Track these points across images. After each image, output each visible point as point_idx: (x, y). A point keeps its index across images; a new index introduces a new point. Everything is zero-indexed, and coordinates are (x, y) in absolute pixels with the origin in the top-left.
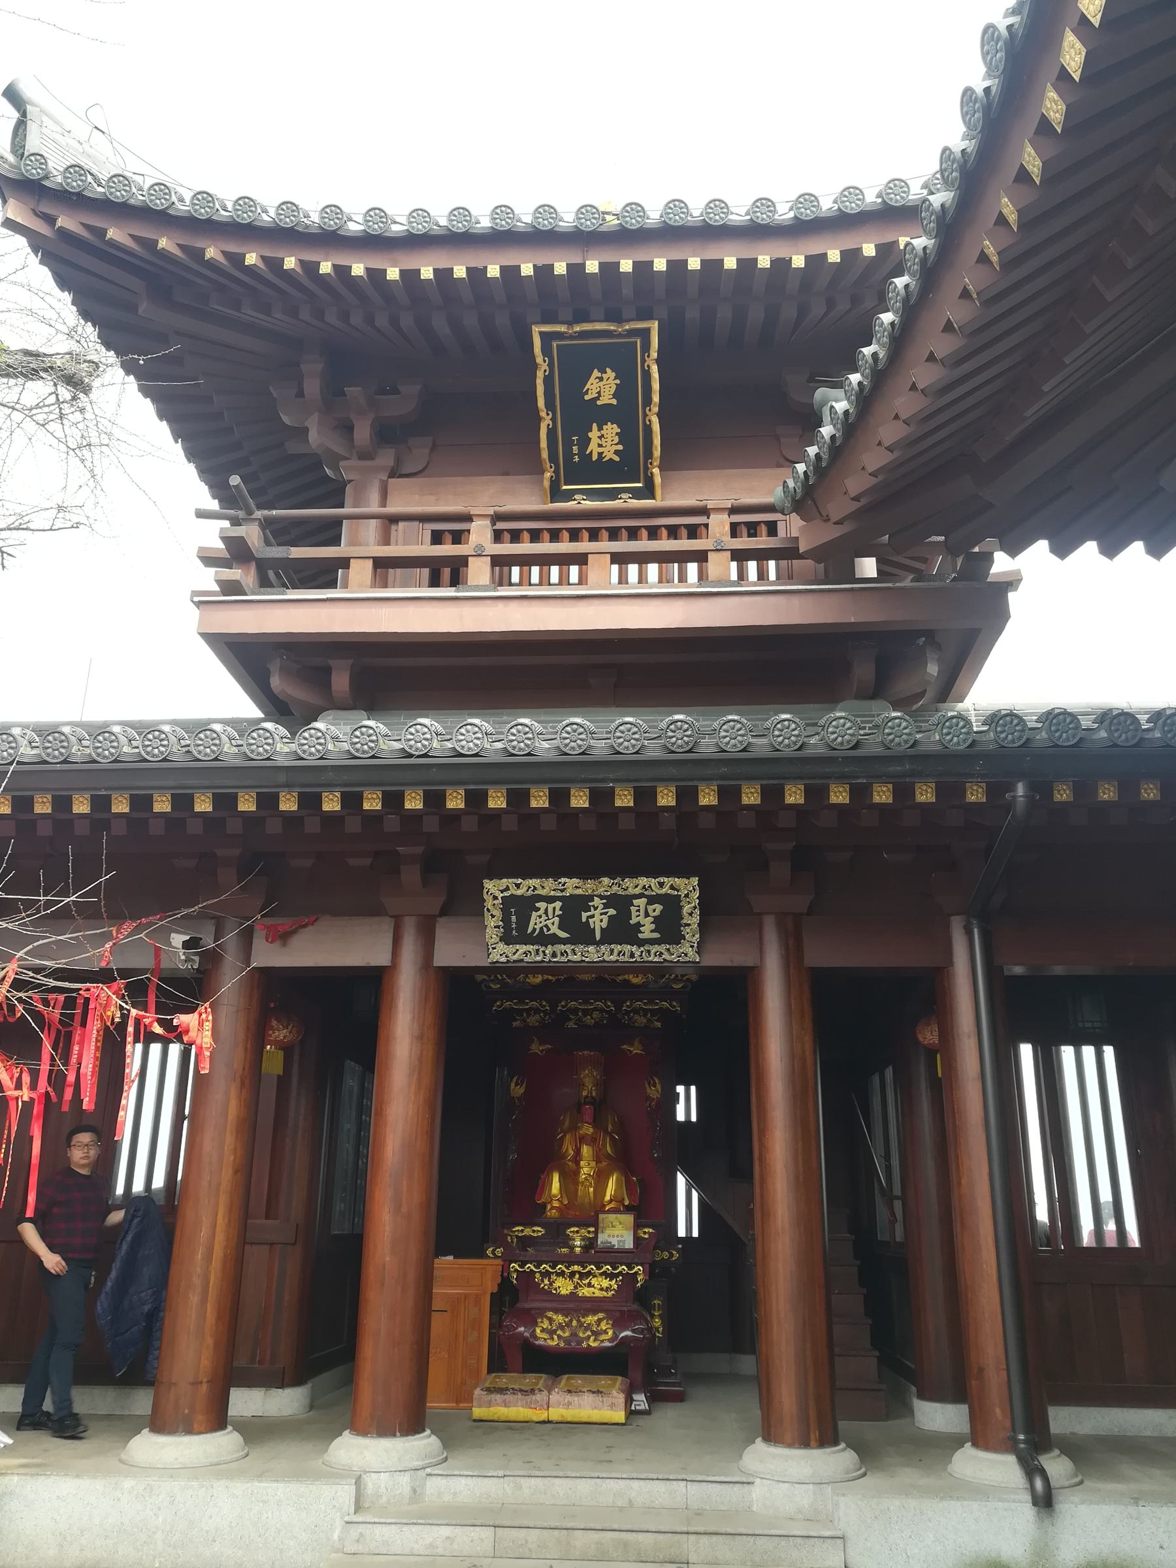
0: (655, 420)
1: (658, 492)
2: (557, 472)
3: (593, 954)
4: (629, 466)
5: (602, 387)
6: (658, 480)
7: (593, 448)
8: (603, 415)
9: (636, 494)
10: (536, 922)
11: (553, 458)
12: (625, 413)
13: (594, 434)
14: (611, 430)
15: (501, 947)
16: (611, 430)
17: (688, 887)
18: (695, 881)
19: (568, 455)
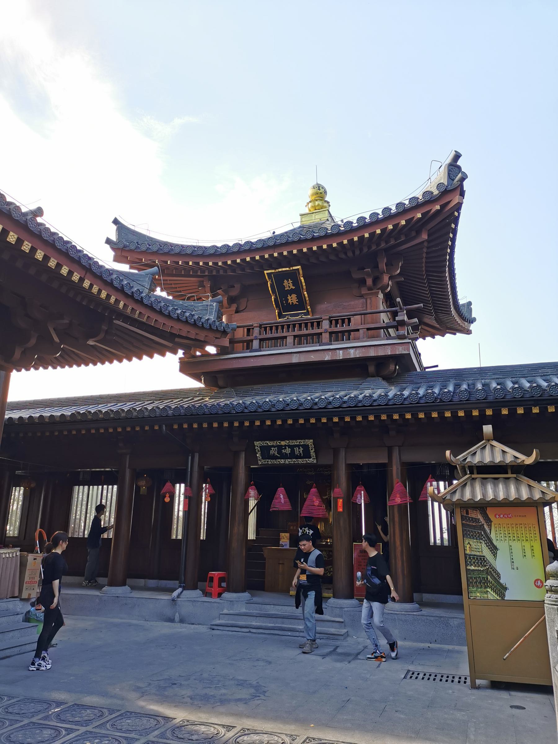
0: (305, 293)
1: (311, 313)
2: (280, 310)
3: (287, 461)
4: (301, 305)
5: (288, 284)
6: (310, 310)
7: (290, 301)
8: (291, 292)
9: (305, 314)
10: (272, 452)
11: (277, 305)
12: (297, 291)
13: (289, 297)
14: (294, 296)
15: (263, 461)
16: (294, 296)
17: (310, 442)
18: (312, 441)
19: (282, 303)
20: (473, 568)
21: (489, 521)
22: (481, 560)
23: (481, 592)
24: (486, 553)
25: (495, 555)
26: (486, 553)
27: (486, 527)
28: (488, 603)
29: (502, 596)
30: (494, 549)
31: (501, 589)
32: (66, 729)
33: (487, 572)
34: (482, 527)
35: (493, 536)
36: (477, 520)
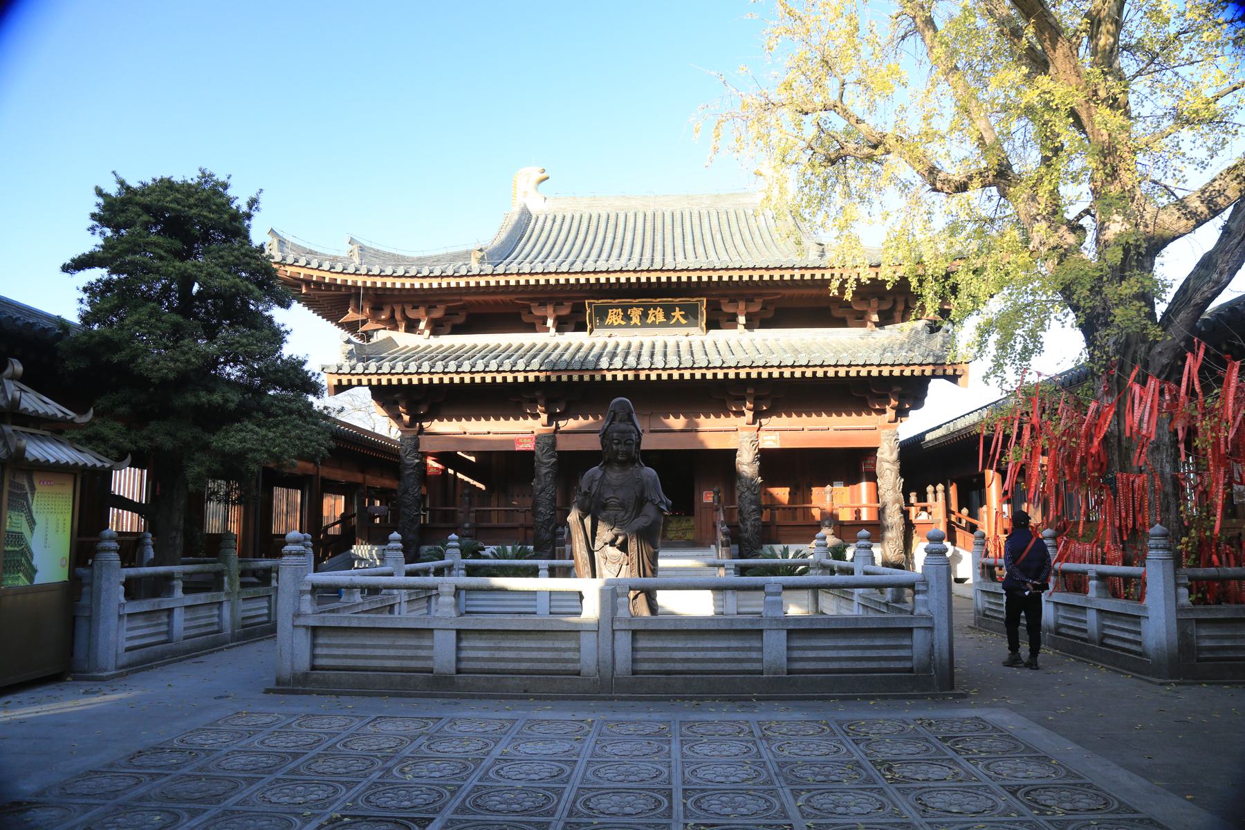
20: (9, 548)
21: (33, 489)
22: (18, 538)
23: (13, 579)
24: (25, 529)
25: (32, 530)
26: (25, 529)
27: (29, 496)
28: (25, 591)
29: (31, 579)
30: (32, 523)
31: (31, 572)
32: (188, 810)
33: (22, 553)
34: (25, 497)
35: (34, 508)
36: (22, 487)
